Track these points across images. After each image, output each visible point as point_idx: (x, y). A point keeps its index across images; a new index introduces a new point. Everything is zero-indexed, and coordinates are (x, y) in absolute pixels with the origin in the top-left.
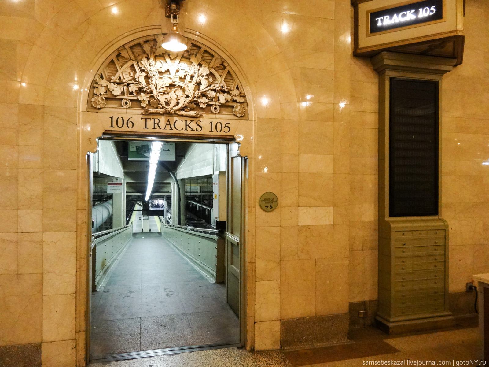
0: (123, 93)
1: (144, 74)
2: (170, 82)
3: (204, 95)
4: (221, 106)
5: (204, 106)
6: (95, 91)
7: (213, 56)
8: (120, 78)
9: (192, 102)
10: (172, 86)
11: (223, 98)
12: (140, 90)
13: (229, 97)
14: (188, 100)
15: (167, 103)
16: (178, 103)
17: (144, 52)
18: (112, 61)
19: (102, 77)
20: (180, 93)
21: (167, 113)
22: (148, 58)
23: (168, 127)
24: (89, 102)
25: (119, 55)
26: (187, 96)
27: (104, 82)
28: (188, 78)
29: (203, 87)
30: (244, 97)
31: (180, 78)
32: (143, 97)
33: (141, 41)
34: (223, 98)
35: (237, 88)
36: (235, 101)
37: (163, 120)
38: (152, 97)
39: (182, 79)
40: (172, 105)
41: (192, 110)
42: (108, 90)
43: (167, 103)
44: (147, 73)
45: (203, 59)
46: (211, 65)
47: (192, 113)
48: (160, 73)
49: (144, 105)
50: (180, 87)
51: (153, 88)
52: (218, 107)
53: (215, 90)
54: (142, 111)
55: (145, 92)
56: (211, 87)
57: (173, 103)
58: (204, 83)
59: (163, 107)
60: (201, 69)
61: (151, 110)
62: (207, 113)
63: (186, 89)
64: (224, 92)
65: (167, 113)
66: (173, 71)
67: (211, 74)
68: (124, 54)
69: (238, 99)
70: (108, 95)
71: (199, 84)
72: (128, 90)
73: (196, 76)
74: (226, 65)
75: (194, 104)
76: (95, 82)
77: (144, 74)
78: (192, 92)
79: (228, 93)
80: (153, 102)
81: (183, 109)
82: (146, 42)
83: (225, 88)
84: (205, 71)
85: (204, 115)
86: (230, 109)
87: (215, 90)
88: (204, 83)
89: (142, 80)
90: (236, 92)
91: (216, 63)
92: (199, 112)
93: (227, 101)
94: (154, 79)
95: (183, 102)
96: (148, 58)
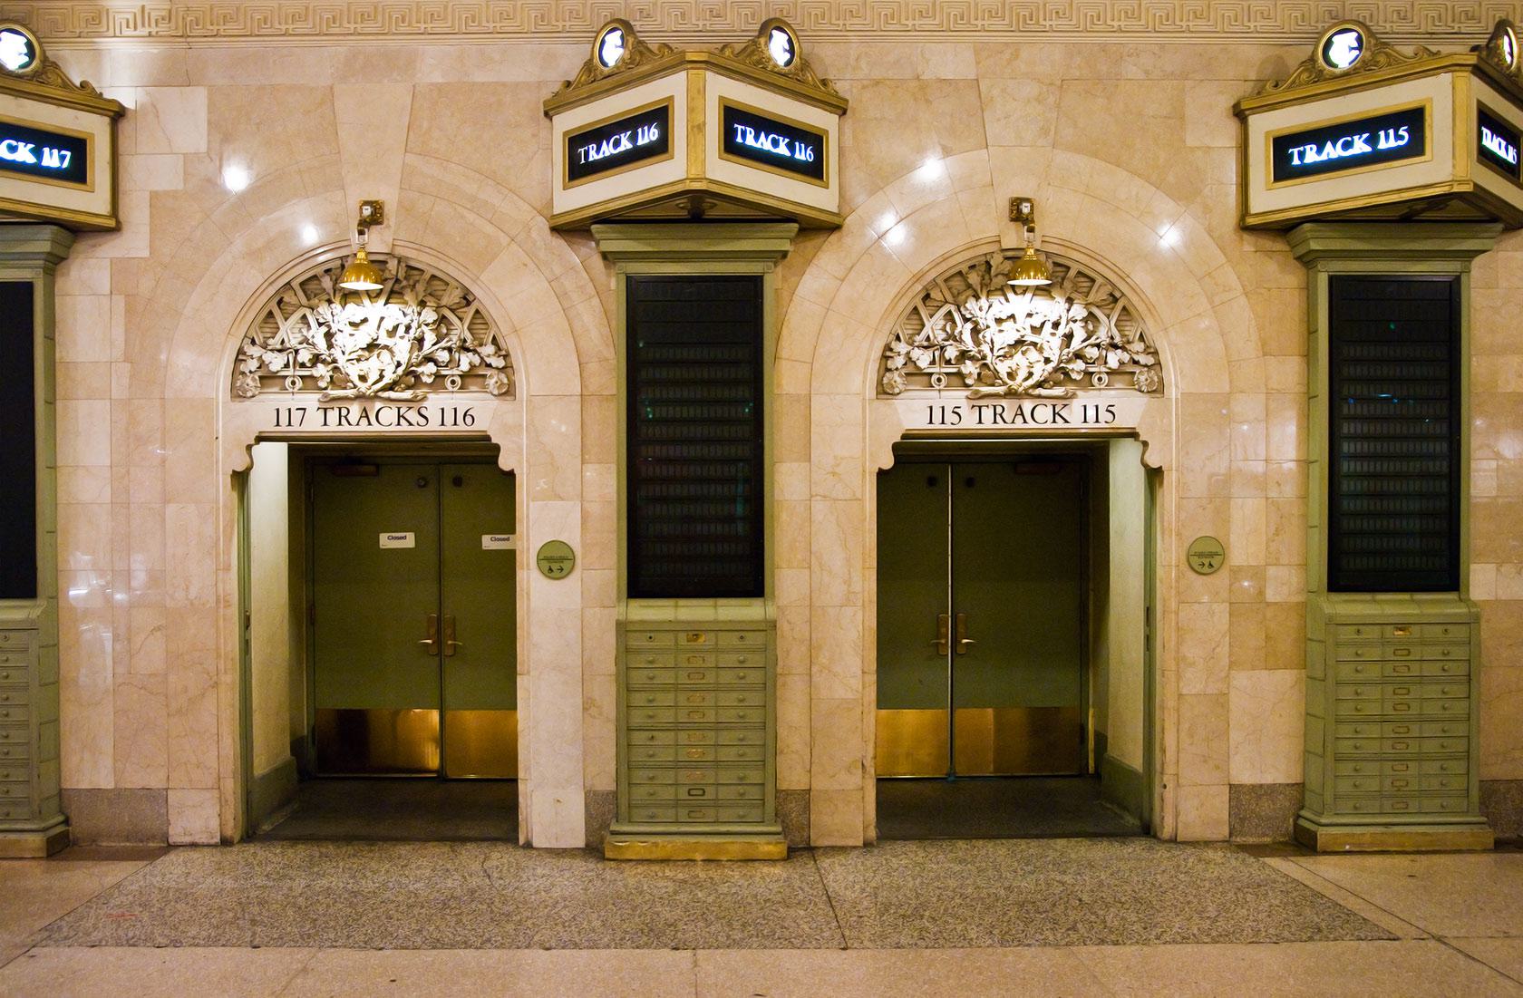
0: (933, 362)
1: (969, 326)
2: (1017, 336)
3: (1078, 355)
4: (1111, 373)
5: (1078, 377)
6: (890, 364)
7: (1093, 281)
8: (928, 339)
9: (1056, 370)
10: (1020, 342)
11: (1114, 359)
12: (964, 356)
13: (1126, 357)
14: (1050, 367)
15: (1011, 375)
16: (1031, 374)
17: (969, 286)
18: (915, 308)
19: (898, 338)
20: (1033, 355)
21: (1011, 394)
22: (977, 298)
23: (1019, 419)
24: (880, 383)
25: (927, 297)
26: (1047, 361)
27: (902, 347)
28: (1048, 326)
29: (1076, 344)
30: (1155, 353)
31: (1033, 328)
32: (970, 368)
33: (964, 268)
34: (1114, 359)
35: (1142, 338)
36: (1136, 363)
37: (1009, 406)
38: (985, 365)
39: (1036, 330)
40: (1019, 379)
41: (1057, 384)
42: (909, 360)
43: (1011, 375)
44: (976, 323)
45: (1076, 289)
46: (1090, 299)
47: (1058, 391)
48: (999, 321)
49: (969, 381)
50: (1034, 344)
51: (986, 348)
52: (1105, 377)
53: (1098, 346)
54: (968, 393)
55: (972, 358)
56: (1092, 341)
57: (1022, 374)
58: (1079, 334)
59: (1005, 384)
60: (1075, 307)
61: (985, 390)
62: (1084, 388)
63: (1046, 346)
64: (1115, 347)
65: (1011, 394)
66: (1020, 317)
67: (1091, 314)
68: (935, 294)
69: (1143, 359)
70: (910, 369)
71: (1069, 337)
72: (942, 355)
73: (1063, 322)
74: (1117, 294)
75: (1061, 375)
76: (888, 348)
77: (969, 326)
78: (1057, 352)
79: (1123, 349)
80: (988, 374)
81: (1039, 385)
82: (972, 267)
83: (1117, 340)
84: (1079, 311)
85: (1079, 393)
86: (1127, 377)
87: (1098, 346)
88: (1079, 334)
89: (967, 337)
90: (1139, 346)
91: (1099, 294)
92: (1070, 388)
93: (1122, 363)
94: (988, 334)
95: (1040, 371)
96: (977, 298)
